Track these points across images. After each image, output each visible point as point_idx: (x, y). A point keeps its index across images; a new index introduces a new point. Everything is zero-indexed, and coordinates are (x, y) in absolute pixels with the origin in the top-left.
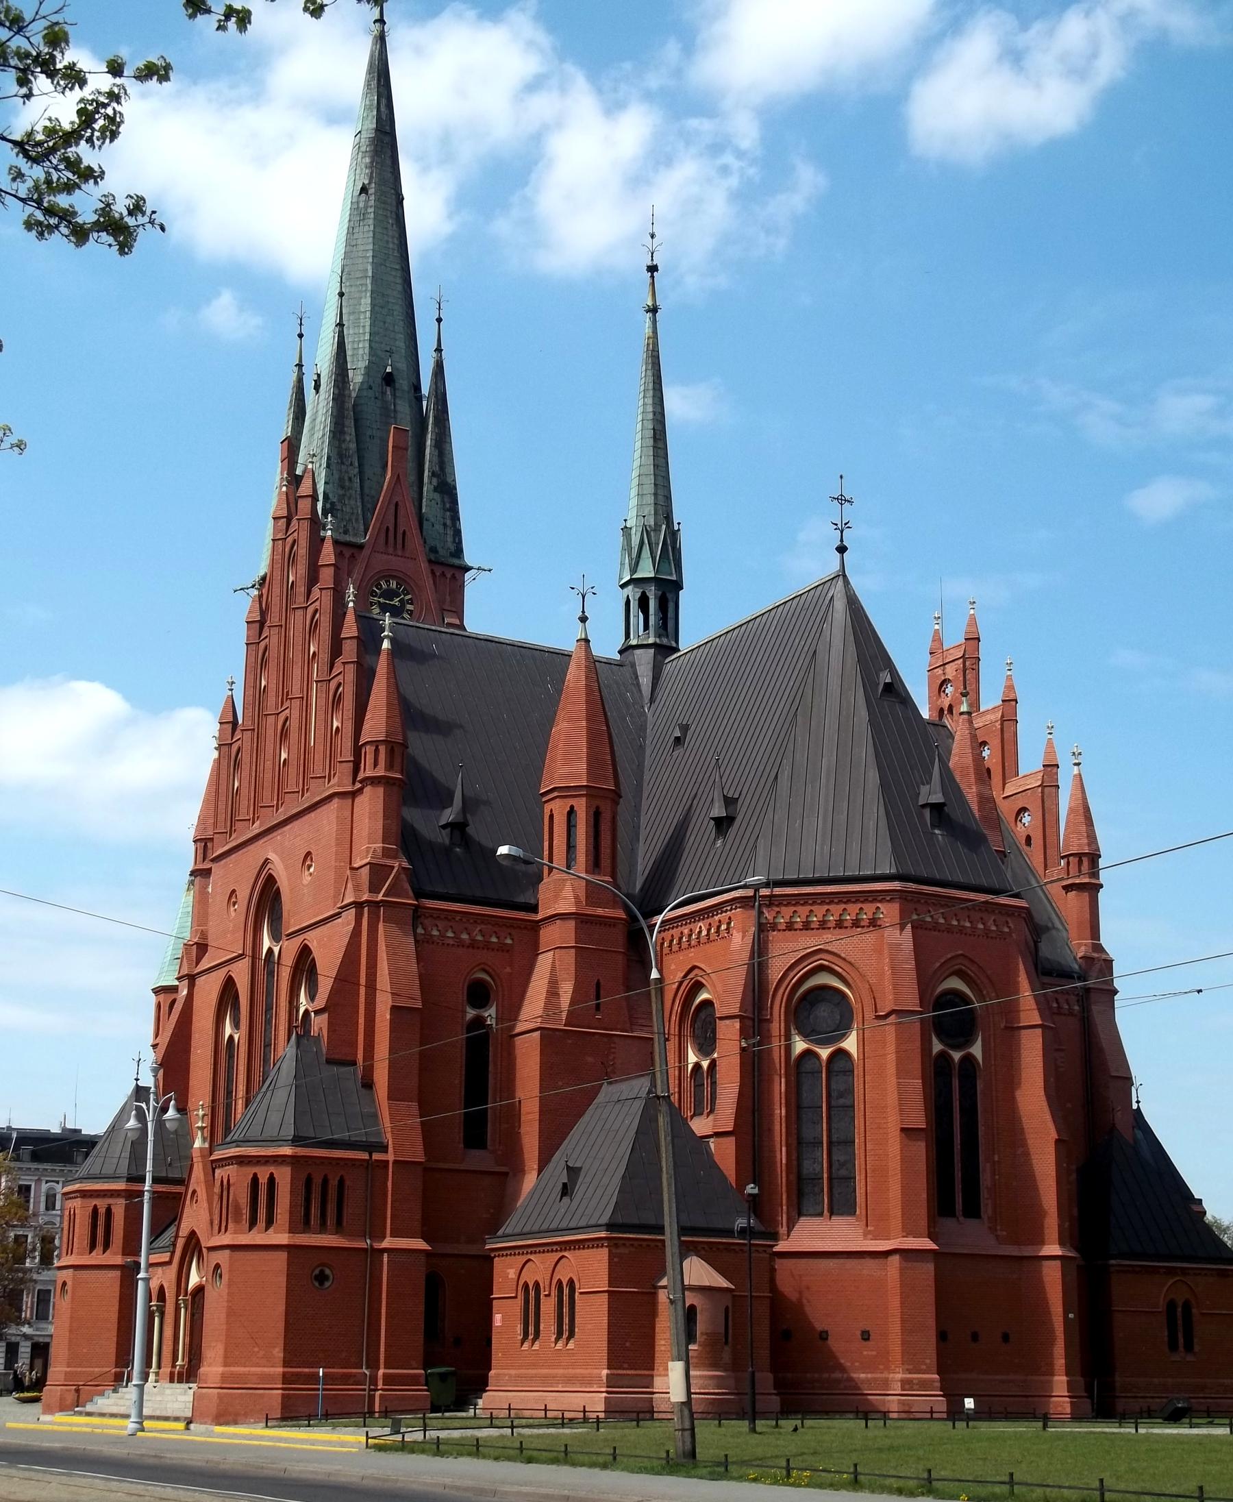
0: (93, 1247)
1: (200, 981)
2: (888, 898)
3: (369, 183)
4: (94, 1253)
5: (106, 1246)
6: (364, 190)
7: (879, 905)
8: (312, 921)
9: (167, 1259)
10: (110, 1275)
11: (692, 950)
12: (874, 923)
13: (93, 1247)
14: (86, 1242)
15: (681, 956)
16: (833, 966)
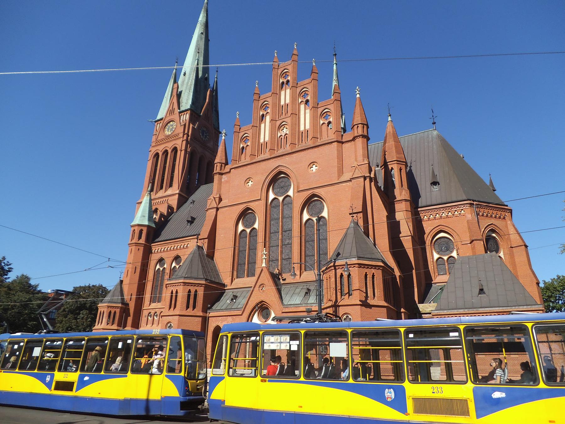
0: (188, 307)
1: (220, 210)
2: (508, 211)
3: (204, 32)
4: (189, 310)
5: (194, 307)
6: (202, 33)
7: (506, 213)
8: (235, 203)
9: (240, 314)
10: (196, 320)
11: (437, 220)
12: (504, 218)
13: (188, 307)
14: (185, 305)
15: (430, 222)
16: (496, 230)
